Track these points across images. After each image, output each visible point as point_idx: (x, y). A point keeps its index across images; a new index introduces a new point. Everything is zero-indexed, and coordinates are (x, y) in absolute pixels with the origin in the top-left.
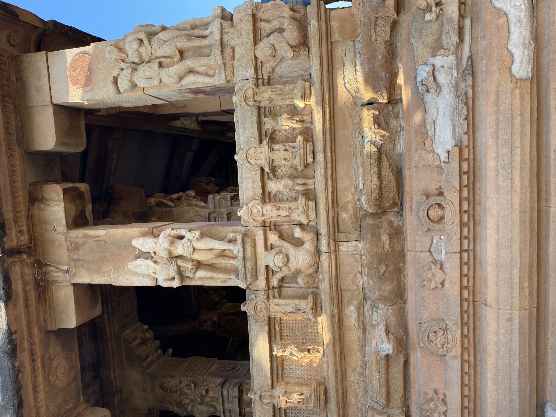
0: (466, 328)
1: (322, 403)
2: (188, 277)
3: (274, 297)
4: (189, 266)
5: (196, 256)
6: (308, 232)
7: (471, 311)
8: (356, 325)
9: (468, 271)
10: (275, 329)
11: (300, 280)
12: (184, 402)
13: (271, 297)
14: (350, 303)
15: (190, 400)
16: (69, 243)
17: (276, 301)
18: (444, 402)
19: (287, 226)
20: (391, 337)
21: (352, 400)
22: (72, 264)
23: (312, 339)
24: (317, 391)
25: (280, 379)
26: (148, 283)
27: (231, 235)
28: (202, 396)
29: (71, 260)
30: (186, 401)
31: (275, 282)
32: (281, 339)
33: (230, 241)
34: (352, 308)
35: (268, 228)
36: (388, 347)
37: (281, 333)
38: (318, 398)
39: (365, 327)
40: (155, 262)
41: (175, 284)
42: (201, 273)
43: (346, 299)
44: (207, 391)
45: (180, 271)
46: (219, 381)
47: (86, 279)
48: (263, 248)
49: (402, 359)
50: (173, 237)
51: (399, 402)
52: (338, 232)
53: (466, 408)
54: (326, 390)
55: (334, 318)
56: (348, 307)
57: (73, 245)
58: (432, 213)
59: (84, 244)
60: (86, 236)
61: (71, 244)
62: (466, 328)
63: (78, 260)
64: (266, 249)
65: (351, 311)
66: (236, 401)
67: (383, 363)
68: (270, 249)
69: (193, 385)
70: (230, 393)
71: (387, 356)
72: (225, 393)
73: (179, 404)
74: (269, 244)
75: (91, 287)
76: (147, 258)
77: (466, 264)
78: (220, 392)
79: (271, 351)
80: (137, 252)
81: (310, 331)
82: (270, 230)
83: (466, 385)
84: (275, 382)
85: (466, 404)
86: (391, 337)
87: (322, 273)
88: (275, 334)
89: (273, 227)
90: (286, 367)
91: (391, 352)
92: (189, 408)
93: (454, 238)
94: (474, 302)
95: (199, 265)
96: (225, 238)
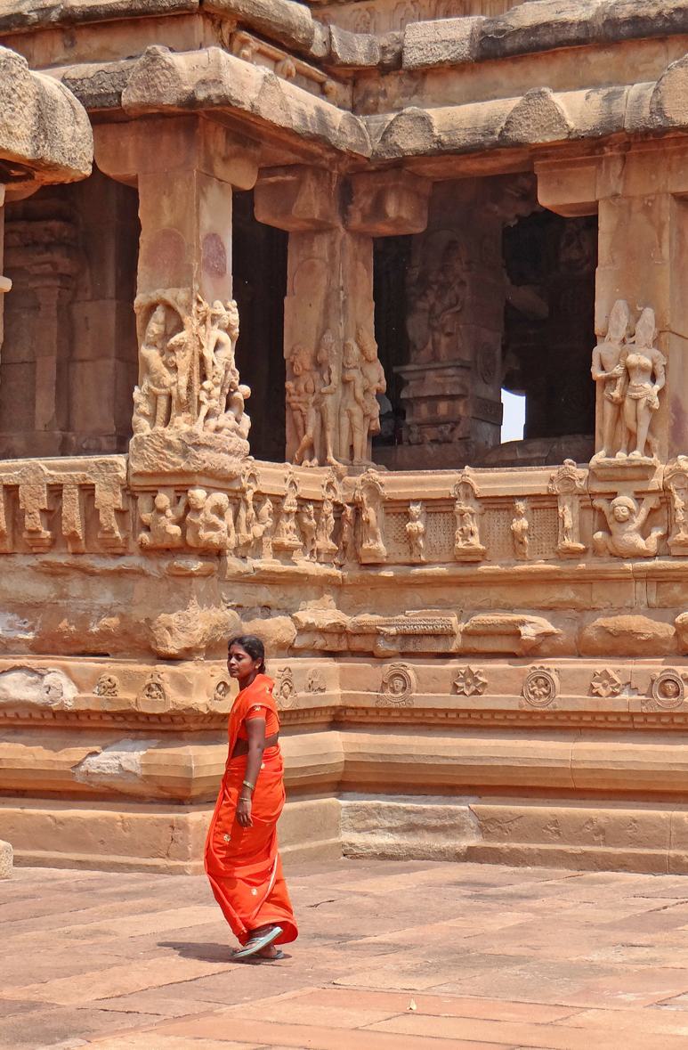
0: (552, 717)
1: (463, 558)
2: (604, 387)
3: (581, 501)
4: (616, 394)
5: (628, 403)
6: (658, 545)
7: (570, 724)
8: (552, 600)
9: (611, 722)
10: (544, 501)
11: (599, 535)
12: (428, 292)
13: (580, 498)
14: (577, 592)
15: (434, 305)
16: (653, 197)
17: (577, 504)
18: (476, 693)
19: (666, 518)
20: (540, 640)
21: (467, 592)
22: (624, 202)
23: (534, 547)
24: (477, 552)
25: (487, 506)
26: (599, 327)
27: (655, 444)
28: (443, 327)
29: (630, 198)
30: (432, 298)
31: (600, 503)
32: (533, 509)
33: (648, 444)
34: (572, 595)
35: (662, 495)
36: (528, 632)
37: (540, 509)
38: (468, 553)
39: (551, 609)
40: (623, 341)
41: (597, 374)
42: (609, 408)
43: (582, 588)
44: (449, 335)
45: (611, 380)
46: (467, 357)
47: (605, 224)
48: (637, 490)
49: (517, 650)
50: (653, 368)
51: (470, 646)
52: (658, 582)
53: (470, 715)
54: (479, 562)
55: (559, 575)
56: (573, 590)
57: (650, 204)
58: (670, 685)
59: (651, 222)
60: (662, 225)
61: (652, 201)
62: (552, 717)
63: (630, 212)
64: (636, 493)
65: (568, 594)
66: (439, 392)
67: (511, 629)
68: (637, 497)
69: (457, 308)
70: (449, 380)
71: (519, 634)
72: (451, 372)
73: (423, 281)
74: (643, 496)
75: (596, 217)
76: (628, 328)
77: (619, 719)
78: (450, 364)
79: (521, 498)
80: (639, 309)
81: (544, 544)
82: (660, 498)
83: (493, 717)
84: (483, 501)
85: (473, 716)
86: (540, 640)
87: (610, 562)
88: (539, 502)
89: (664, 500)
90: (501, 513)
91: (524, 637)
92: (420, 305)
93: (644, 708)
94: (581, 728)
95: (619, 405)
96: (654, 436)
